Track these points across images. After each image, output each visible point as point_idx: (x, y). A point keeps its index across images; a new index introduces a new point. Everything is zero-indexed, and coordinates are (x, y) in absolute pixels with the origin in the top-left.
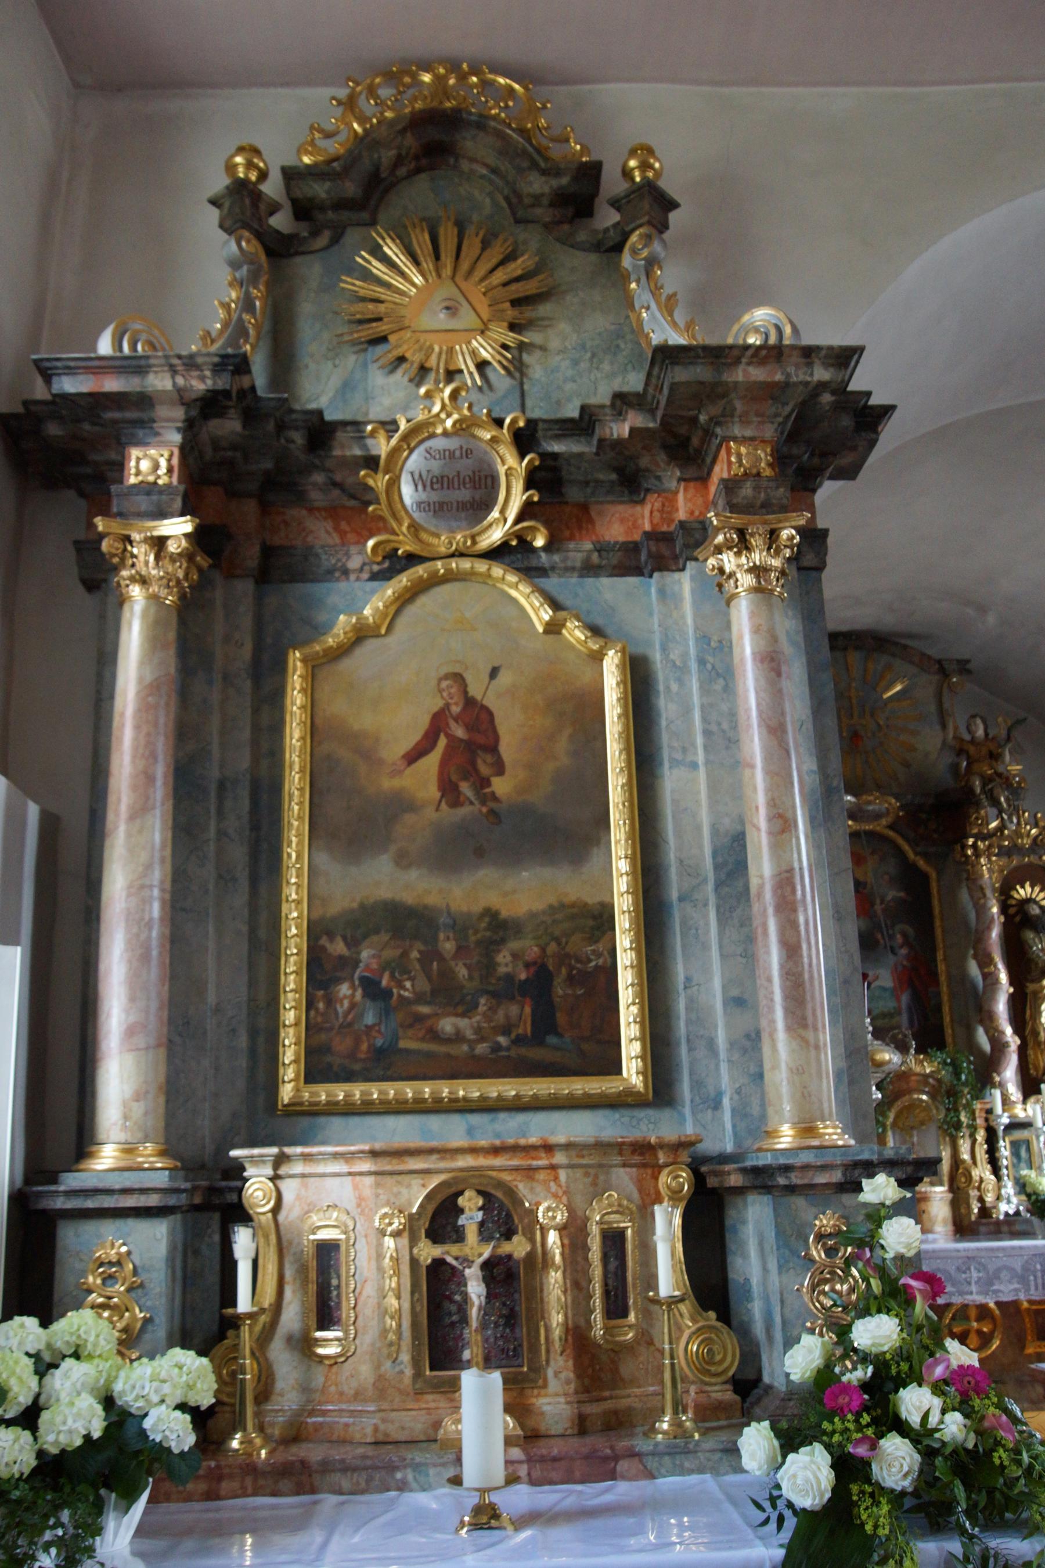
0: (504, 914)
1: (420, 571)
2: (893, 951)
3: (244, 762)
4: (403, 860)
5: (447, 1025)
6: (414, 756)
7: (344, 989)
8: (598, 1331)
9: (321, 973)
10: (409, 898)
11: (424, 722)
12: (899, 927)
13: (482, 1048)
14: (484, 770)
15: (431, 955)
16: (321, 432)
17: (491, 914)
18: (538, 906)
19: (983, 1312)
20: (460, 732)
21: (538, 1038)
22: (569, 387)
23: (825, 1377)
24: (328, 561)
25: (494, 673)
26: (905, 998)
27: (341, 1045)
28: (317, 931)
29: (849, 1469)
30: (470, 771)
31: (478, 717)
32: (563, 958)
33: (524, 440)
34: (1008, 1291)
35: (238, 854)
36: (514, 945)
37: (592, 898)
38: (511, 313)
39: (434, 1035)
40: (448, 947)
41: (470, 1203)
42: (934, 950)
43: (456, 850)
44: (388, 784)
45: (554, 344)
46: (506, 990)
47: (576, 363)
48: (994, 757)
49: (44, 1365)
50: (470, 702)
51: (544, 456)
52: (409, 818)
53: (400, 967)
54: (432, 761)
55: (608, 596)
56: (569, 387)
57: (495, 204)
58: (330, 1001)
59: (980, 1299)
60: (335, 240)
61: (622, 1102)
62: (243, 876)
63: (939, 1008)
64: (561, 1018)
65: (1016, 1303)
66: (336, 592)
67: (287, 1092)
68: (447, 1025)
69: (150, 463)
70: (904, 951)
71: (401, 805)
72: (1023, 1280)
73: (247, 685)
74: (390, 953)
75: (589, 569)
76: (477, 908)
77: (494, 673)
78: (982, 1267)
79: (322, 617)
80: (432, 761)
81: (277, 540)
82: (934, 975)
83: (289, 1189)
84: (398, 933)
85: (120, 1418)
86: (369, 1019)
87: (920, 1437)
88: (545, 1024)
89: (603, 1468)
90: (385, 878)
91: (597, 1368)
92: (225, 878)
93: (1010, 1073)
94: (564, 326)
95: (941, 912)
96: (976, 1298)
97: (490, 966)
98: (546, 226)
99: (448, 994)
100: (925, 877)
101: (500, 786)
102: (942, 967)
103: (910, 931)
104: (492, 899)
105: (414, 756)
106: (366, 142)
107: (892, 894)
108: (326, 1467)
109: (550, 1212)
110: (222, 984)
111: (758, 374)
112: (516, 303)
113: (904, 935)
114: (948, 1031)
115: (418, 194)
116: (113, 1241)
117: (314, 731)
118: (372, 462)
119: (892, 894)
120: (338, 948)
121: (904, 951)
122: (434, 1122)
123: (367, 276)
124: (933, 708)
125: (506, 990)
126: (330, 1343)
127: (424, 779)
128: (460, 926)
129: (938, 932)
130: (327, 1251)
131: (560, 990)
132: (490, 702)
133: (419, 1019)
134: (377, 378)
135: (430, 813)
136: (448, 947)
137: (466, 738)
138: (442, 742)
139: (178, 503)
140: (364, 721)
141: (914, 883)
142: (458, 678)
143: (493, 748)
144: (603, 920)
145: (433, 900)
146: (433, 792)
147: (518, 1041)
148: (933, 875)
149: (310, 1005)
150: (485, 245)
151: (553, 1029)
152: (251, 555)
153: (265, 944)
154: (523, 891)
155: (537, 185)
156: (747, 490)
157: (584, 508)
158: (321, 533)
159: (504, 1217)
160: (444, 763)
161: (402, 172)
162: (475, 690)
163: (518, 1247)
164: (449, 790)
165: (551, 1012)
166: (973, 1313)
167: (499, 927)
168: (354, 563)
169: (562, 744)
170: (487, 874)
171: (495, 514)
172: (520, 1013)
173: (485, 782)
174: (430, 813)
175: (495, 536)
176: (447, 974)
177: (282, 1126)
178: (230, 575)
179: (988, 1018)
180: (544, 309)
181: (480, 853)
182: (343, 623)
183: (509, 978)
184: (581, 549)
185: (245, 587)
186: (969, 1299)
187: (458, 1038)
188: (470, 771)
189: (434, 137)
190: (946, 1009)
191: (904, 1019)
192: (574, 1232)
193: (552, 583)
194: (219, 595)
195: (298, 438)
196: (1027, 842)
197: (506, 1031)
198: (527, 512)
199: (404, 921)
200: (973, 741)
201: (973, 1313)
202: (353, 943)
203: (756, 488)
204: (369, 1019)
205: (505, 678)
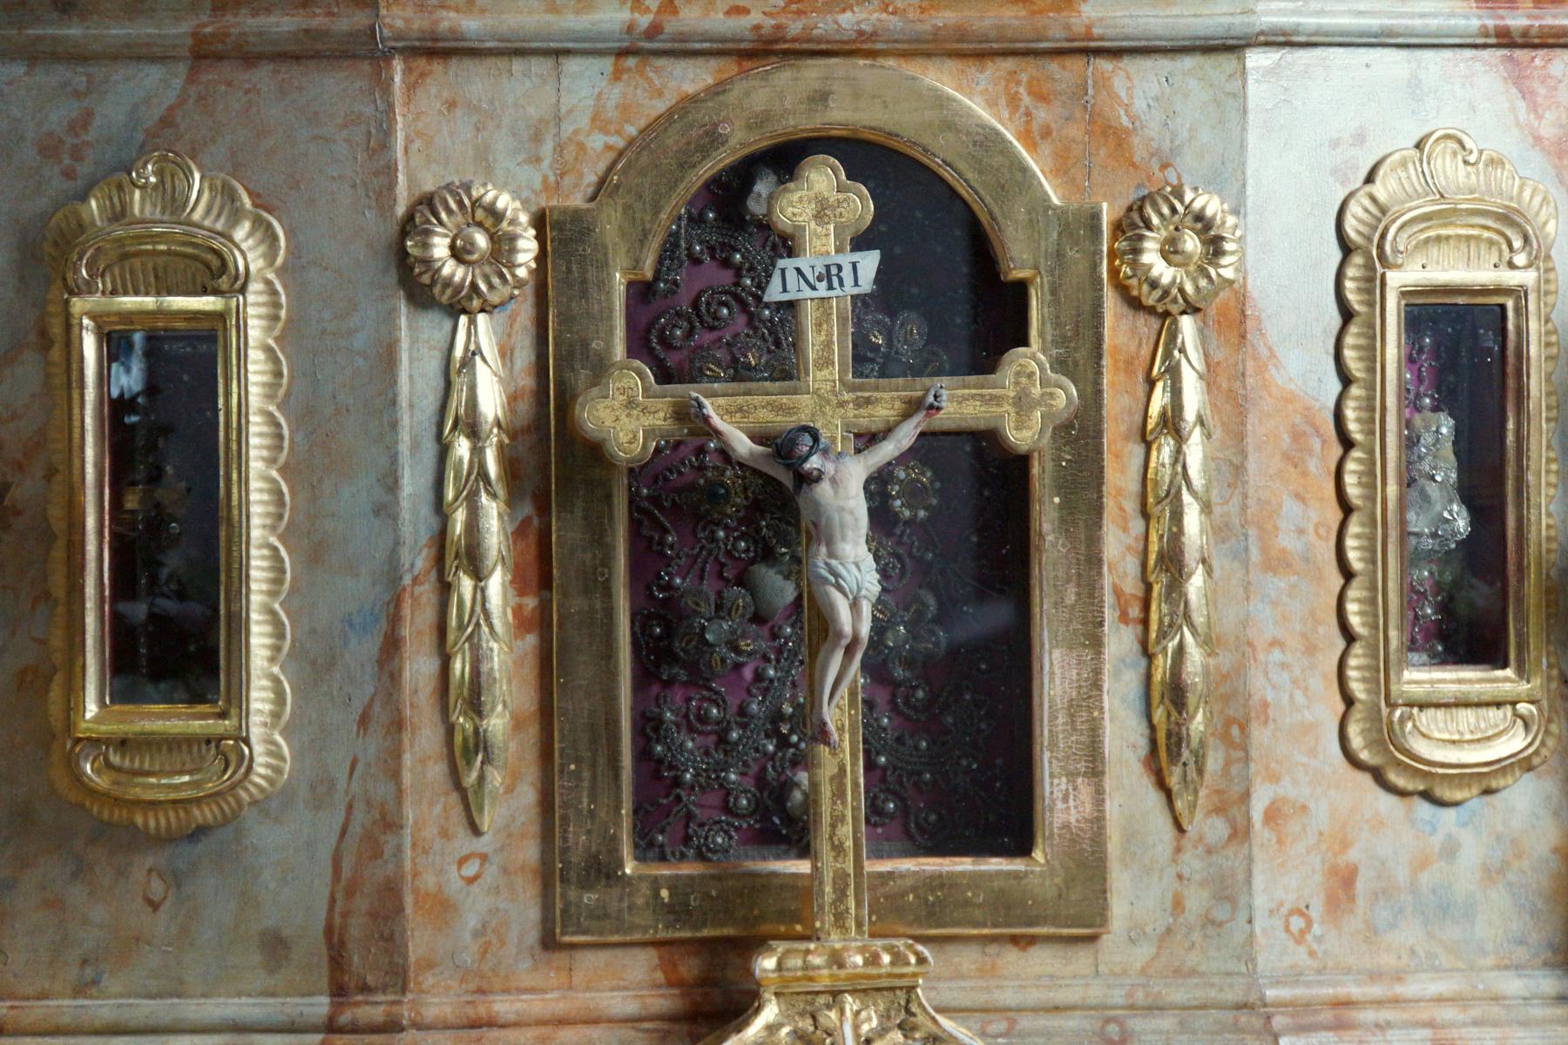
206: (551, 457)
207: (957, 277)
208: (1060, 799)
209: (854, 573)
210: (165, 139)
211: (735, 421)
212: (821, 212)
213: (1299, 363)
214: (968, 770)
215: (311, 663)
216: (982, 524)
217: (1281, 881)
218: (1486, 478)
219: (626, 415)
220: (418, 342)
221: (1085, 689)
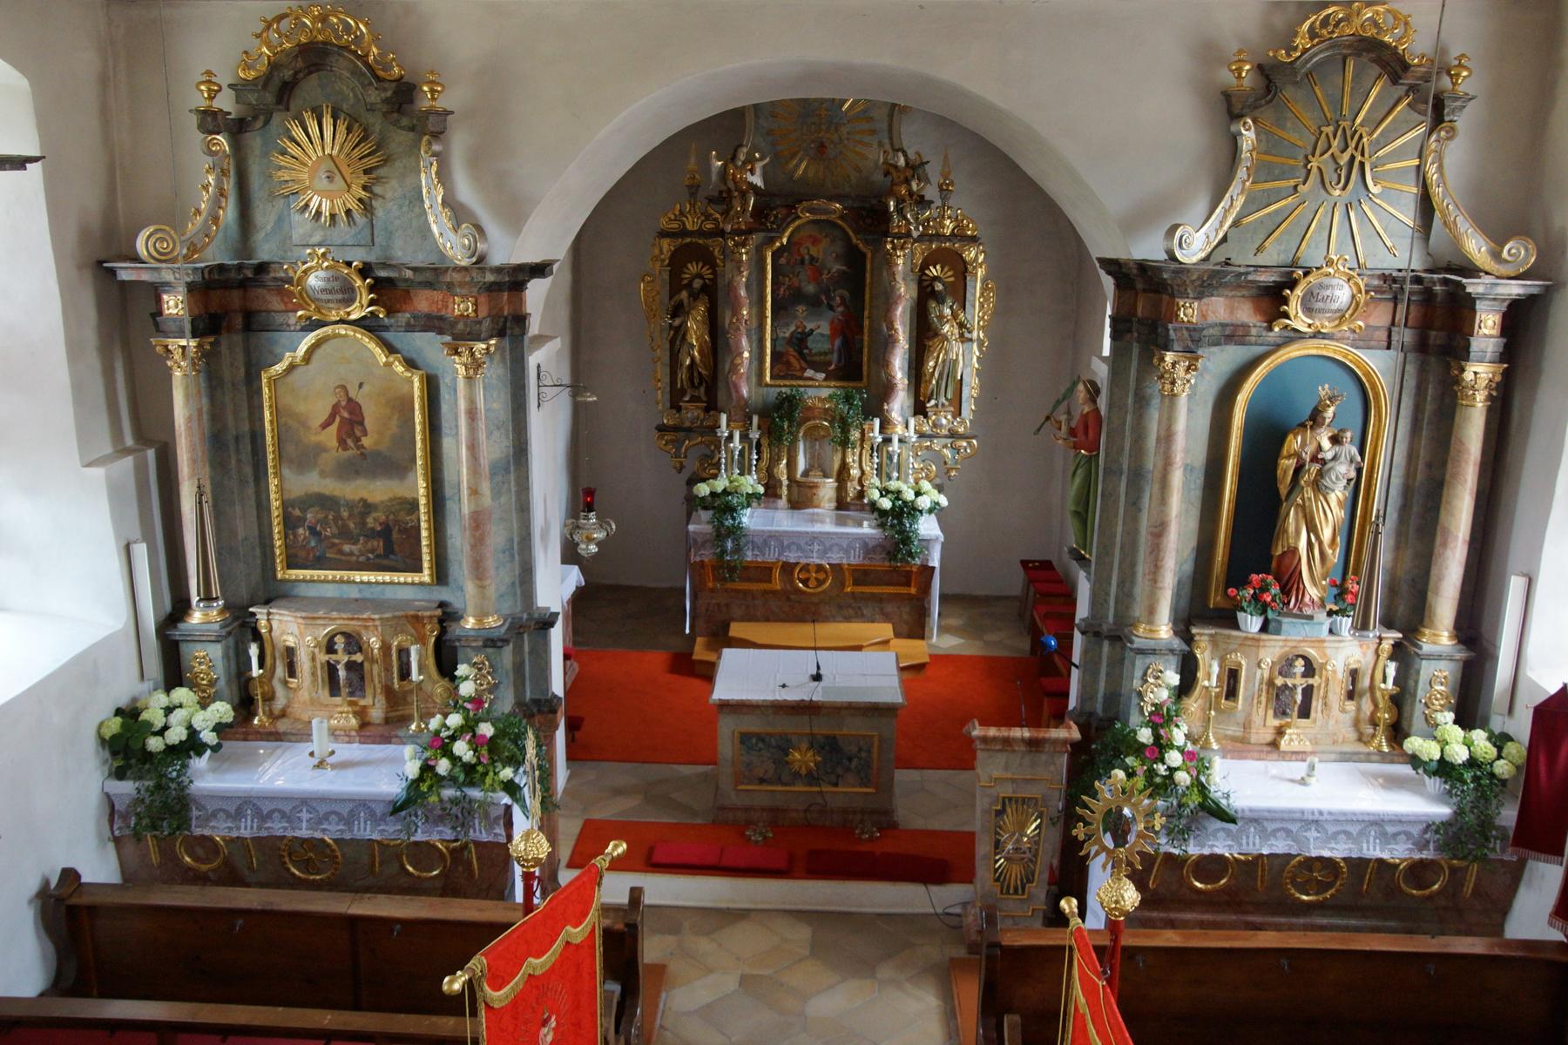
0: (370, 500)
1: (320, 332)
2: (831, 308)
3: (246, 427)
4: (323, 474)
5: (347, 548)
6: (326, 425)
7: (301, 531)
8: (396, 686)
9: (289, 523)
10: (327, 492)
11: (329, 409)
12: (840, 291)
13: (362, 559)
14: (358, 433)
15: (338, 517)
16: (262, 268)
17: (364, 501)
18: (385, 498)
19: (820, 568)
20: (346, 415)
21: (386, 556)
22: (397, 222)
23: (437, 733)
24: (279, 319)
25: (361, 385)
26: (838, 342)
27: (302, 554)
28: (286, 505)
29: (427, 769)
30: (352, 434)
31: (354, 407)
32: (397, 522)
33: (365, 271)
34: (836, 557)
35: (248, 470)
36: (374, 515)
37: (409, 495)
38: (364, 179)
39: (341, 552)
40: (345, 514)
41: (339, 640)
42: (863, 309)
43: (348, 470)
44: (314, 439)
45: (389, 195)
46: (371, 534)
47: (401, 207)
48: (907, 181)
49: (169, 710)
50: (350, 400)
51: (377, 280)
52: (324, 455)
53: (324, 522)
54: (334, 428)
55: (418, 343)
56: (397, 222)
57: (355, 96)
58: (295, 536)
59: (818, 561)
60: (267, 122)
61: (422, 584)
62: (251, 480)
63: (861, 352)
64: (396, 548)
65: (840, 565)
66: (283, 338)
67: (279, 576)
68: (347, 548)
69: (174, 305)
70: (840, 309)
71: (321, 448)
72: (847, 551)
73: (244, 389)
74: (320, 516)
75: (410, 328)
76: (357, 498)
77: (361, 385)
78: (821, 543)
79: (278, 350)
80: (334, 428)
81: (255, 306)
82: (861, 327)
83: (275, 624)
84: (323, 507)
85: (193, 732)
86: (313, 544)
87: (455, 760)
88: (389, 550)
89: (386, 740)
90: (313, 482)
91: (394, 699)
92: (243, 482)
93: (899, 405)
94: (394, 183)
95: (872, 283)
96: (816, 560)
97: (364, 524)
98: (385, 115)
99: (345, 534)
100: (864, 255)
101: (366, 441)
102: (866, 322)
103: (846, 293)
104: (365, 494)
105: (326, 425)
106: (274, 66)
107: (837, 267)
108: (285, 734)
109: (375, 642)
110: (244, 528)
111: (457, 277)
112: (366, 172)
113: (842, 298)
114: (865, 368)
115: (311, 88)
116: (199, 651)
117: (277, 411)
118: (290, 281)
119: (837, 267)
120: (297, 512)
121: (840, 309)
122: (345, 587)
123: (284, 153)
124: (885, 126)
125: (371, 534)
126: (293, 682)
127: (330, 437)
128: (350, 506)
129: (867, 296)
130: (290, 652)
131: (395, 535)
132: (360, 400)
133: (334, 545)
134: (296, 217)
135: (334, 453)
136: (345, 514)
137: (349, 418)
138: (338, 419)
139: (188, 327)
140: (301, 408)
141: (854, 260)
142: (344, 387)
143: (361, 423)
144: (413, 505)
145: (337, 493)
146: (334, 443)
147: (378, 556)
148: (869, 255)
149: (286, 537)
150: (349, 130)
151: (393, 552)
152: (238, 321)
153: (262, 506)
154: (379, 490)
155: (374, 96)
156: (461, 326)
157: (408, 292)
158: (276, 303)
159: (354, 642)
160: (339, 430)
161: (301, 75)
162: (352, 394)
163: (358, 658)
164: (342, 442)
165: (392, 544)
166: (813, 569)
167: (367, 507)
168: (292, 321)
169: (394, 423)
170: (361, 482)
171: (357, 304)
172: (378, 544)
173: (359, 440)
174: (334, 453)
175: (353, 317)
176: (345, 526)
177: (274, 594)
178: (230, 330)
179: (886, 364)
180: (382, 172)
181: (357, 473)
182: (287, 359)
183: (373, 529)
184: (403, 317)
185: (238, 338)
186: (809, 561)
187: (351, 554)
188: (352, 434)
189: (314, 57)
190: (865, 351)
191: (835, 357)
192: (386, 648)
193: (388, 336)
194: (224, 349)
195: (249, 274)
196: (948, 232)
197: (372, 551)
198: (371, 303)
199: (325, 502)
200: (896, 167)
201: (813, 569)
202: (304, 511)
203: (466, 325)
204: (313, 544)
205: (366, 388)
206: (1271, 683)
207: (1310, 670)
208: (1313, 714)
209: (1299, 698)
210: (1235, 651)
211: (1290, 682)
212: (1299, 666)
213: (1340, 675)
214: (1305, 712)
215: (1245, 700)
216: (1308, 692)
217: (1332, 722)
218: (1354, 683)
219: (1279, 681)
220: (1259, 672)
221: (1316, 704)
